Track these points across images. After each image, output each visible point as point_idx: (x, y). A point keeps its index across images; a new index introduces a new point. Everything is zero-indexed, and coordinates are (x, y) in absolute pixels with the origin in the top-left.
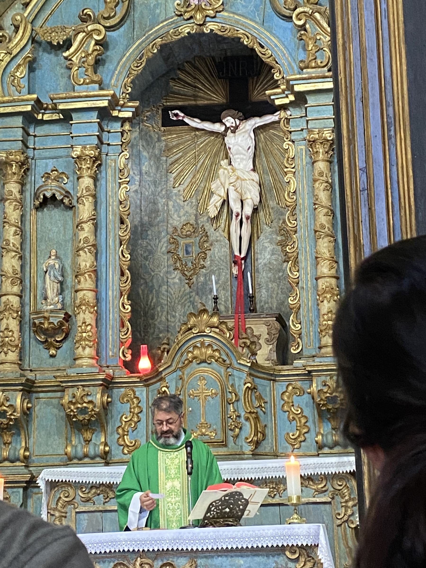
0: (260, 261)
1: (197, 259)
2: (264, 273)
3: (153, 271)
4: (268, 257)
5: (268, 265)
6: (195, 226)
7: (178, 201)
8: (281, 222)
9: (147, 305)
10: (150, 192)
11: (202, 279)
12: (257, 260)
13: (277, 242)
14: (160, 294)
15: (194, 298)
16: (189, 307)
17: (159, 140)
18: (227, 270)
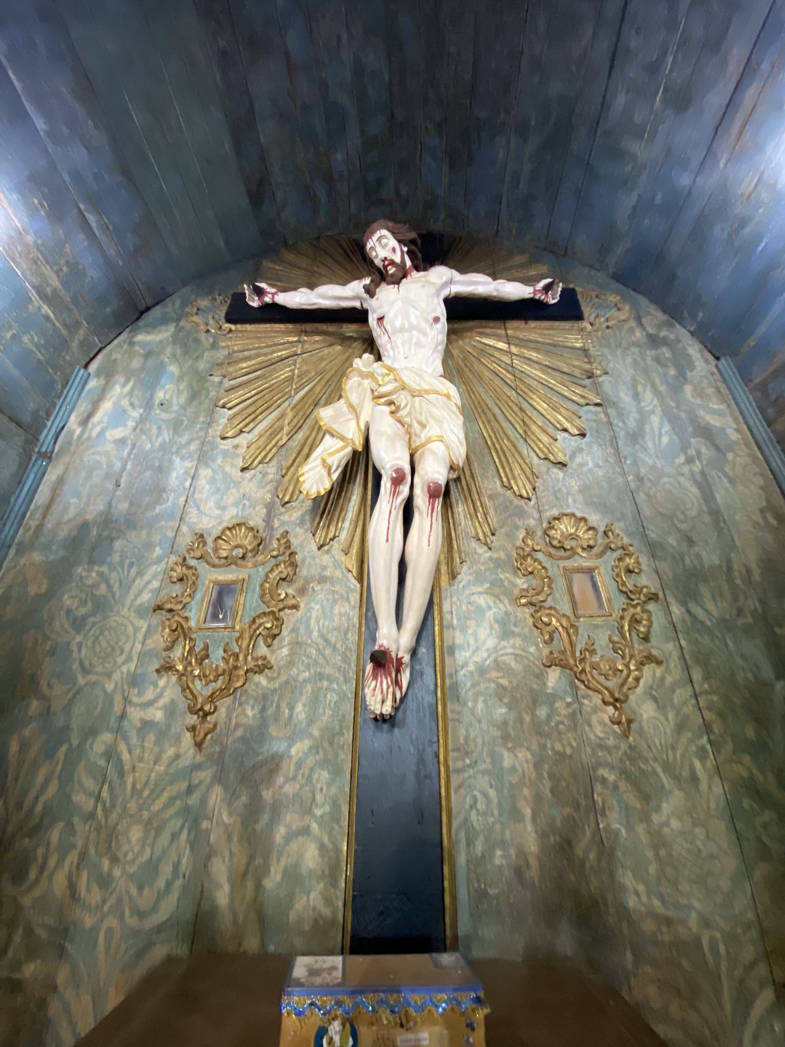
0: (462, 656)
1: (247, 635)
2: (480, 705)
3: (85, 671)
4: (491, 643)
5: (494, 674)
6: (262, 534)
7: (228, 469)
8: (521, 534)
9: (19, 805)
10: (157, 445)
11: (250, 713)
12: (452, 650)
13: (516, 592)
14: (81, 768)
15: (204, 800)
16: (175, 836)
17: (214, 346)
18: (346, 681)
